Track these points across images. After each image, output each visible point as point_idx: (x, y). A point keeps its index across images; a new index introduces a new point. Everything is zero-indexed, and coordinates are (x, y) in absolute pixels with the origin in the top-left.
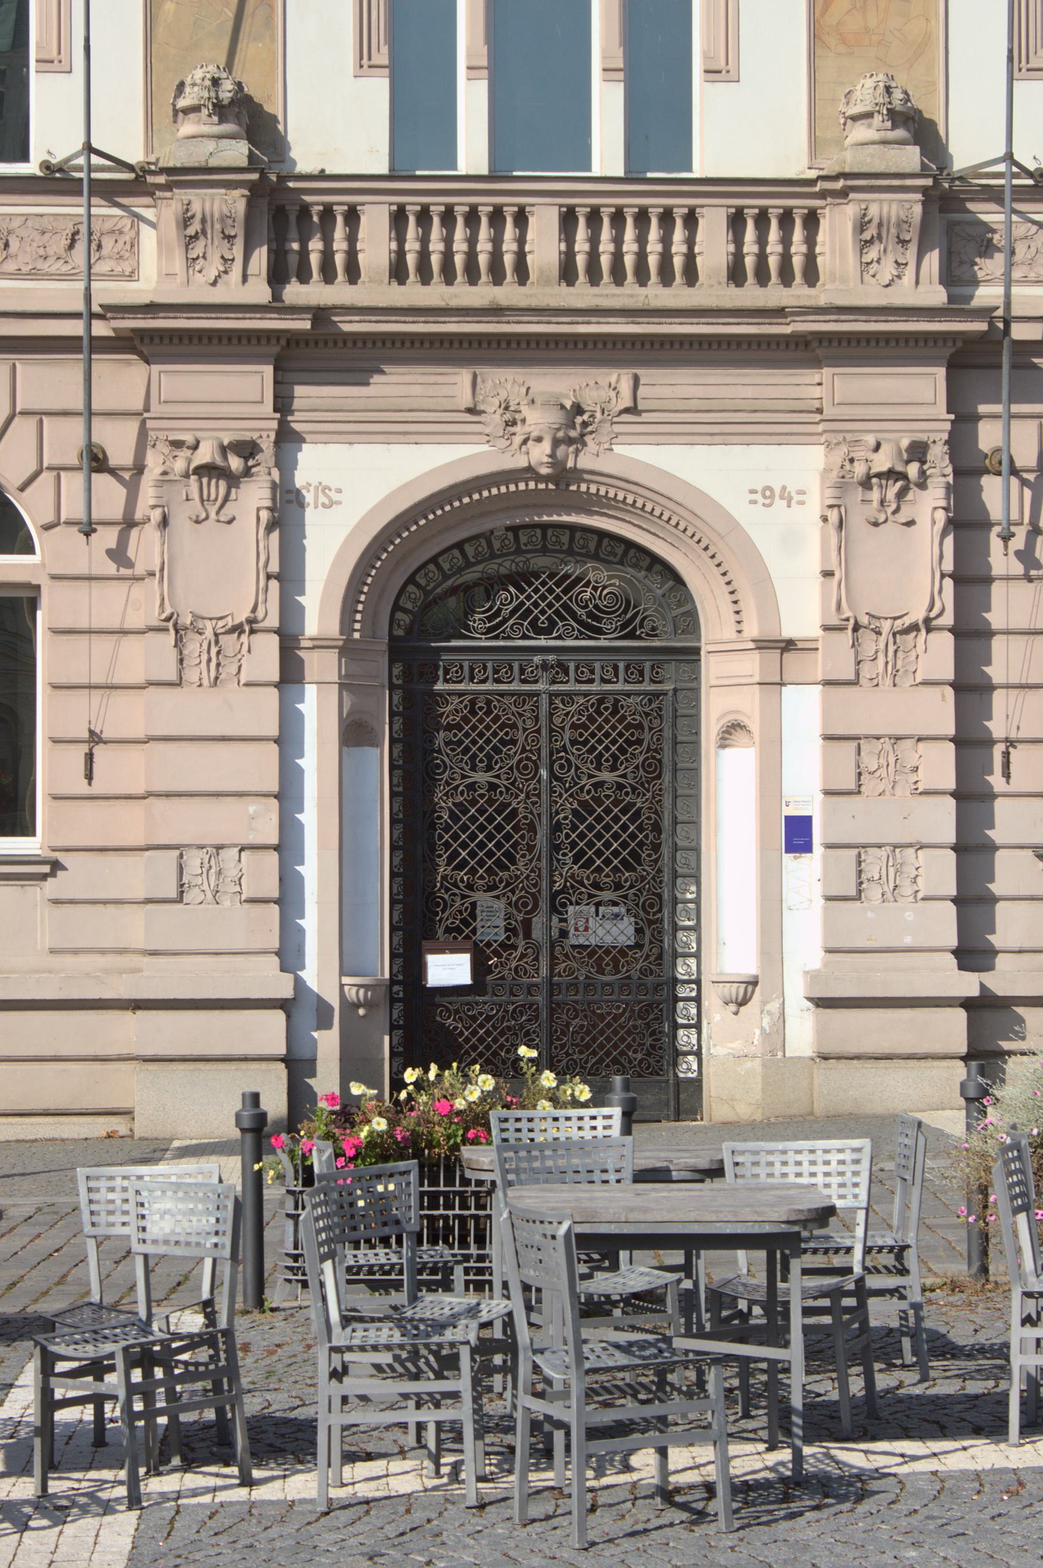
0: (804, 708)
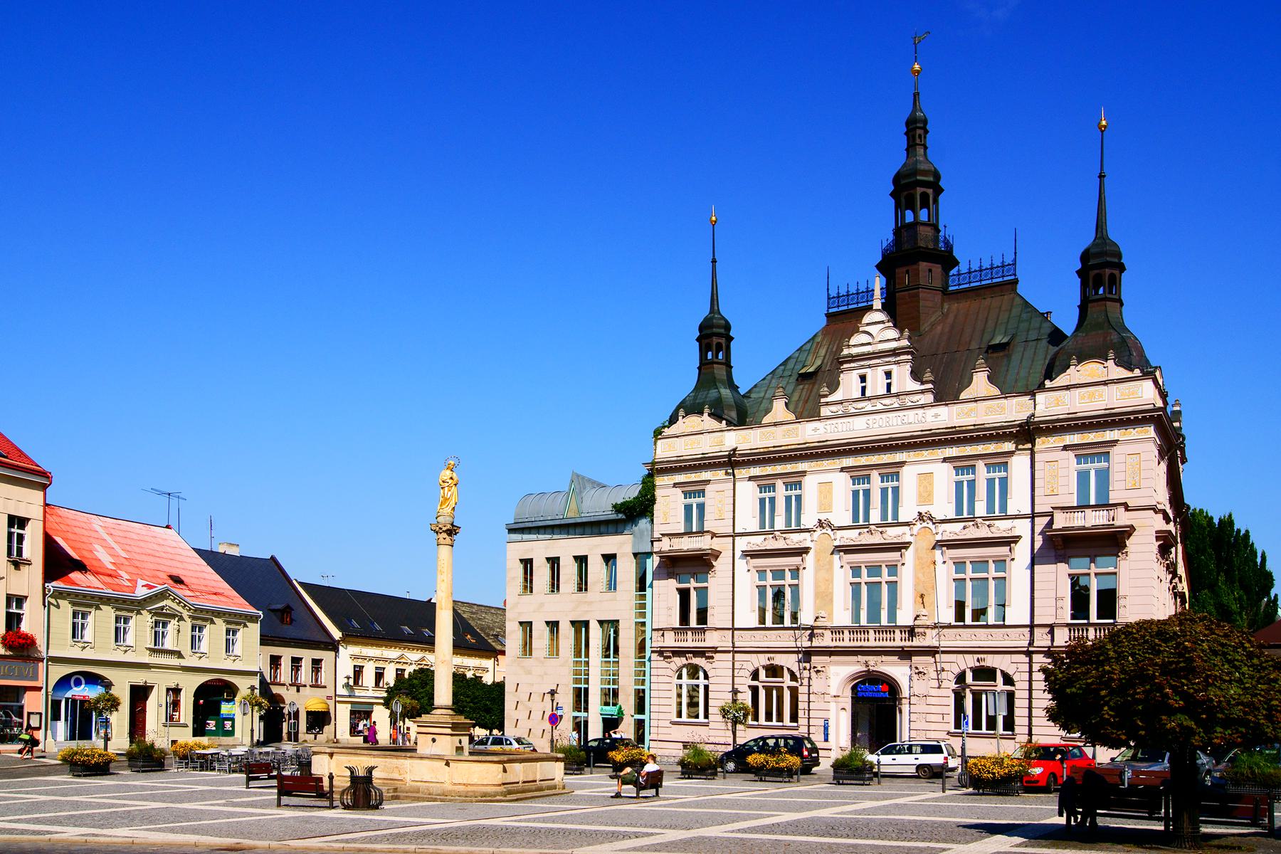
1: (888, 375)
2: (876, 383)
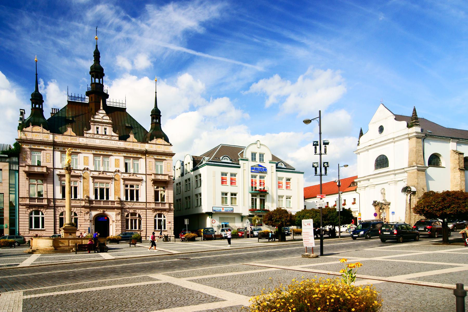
0: (114, 224)
1: (105, 129)
2: (101, 131)
